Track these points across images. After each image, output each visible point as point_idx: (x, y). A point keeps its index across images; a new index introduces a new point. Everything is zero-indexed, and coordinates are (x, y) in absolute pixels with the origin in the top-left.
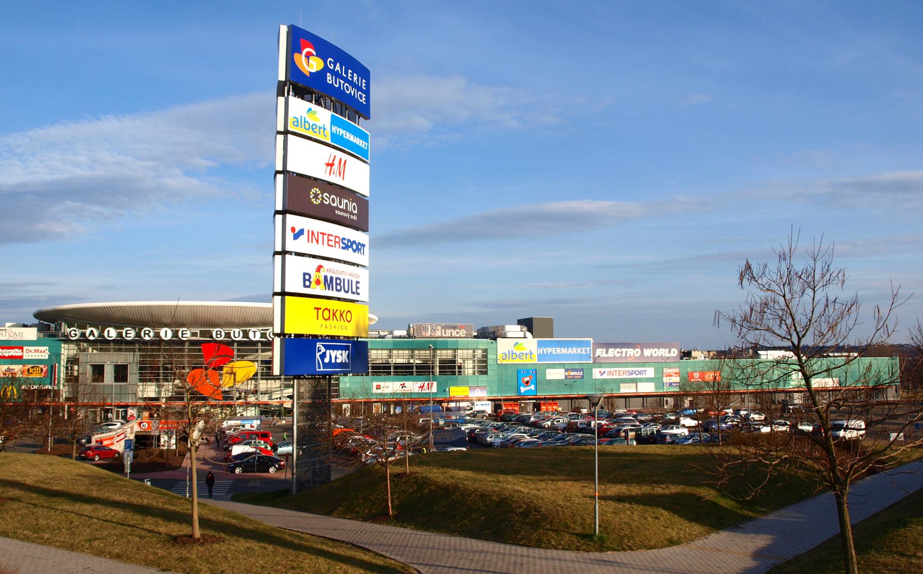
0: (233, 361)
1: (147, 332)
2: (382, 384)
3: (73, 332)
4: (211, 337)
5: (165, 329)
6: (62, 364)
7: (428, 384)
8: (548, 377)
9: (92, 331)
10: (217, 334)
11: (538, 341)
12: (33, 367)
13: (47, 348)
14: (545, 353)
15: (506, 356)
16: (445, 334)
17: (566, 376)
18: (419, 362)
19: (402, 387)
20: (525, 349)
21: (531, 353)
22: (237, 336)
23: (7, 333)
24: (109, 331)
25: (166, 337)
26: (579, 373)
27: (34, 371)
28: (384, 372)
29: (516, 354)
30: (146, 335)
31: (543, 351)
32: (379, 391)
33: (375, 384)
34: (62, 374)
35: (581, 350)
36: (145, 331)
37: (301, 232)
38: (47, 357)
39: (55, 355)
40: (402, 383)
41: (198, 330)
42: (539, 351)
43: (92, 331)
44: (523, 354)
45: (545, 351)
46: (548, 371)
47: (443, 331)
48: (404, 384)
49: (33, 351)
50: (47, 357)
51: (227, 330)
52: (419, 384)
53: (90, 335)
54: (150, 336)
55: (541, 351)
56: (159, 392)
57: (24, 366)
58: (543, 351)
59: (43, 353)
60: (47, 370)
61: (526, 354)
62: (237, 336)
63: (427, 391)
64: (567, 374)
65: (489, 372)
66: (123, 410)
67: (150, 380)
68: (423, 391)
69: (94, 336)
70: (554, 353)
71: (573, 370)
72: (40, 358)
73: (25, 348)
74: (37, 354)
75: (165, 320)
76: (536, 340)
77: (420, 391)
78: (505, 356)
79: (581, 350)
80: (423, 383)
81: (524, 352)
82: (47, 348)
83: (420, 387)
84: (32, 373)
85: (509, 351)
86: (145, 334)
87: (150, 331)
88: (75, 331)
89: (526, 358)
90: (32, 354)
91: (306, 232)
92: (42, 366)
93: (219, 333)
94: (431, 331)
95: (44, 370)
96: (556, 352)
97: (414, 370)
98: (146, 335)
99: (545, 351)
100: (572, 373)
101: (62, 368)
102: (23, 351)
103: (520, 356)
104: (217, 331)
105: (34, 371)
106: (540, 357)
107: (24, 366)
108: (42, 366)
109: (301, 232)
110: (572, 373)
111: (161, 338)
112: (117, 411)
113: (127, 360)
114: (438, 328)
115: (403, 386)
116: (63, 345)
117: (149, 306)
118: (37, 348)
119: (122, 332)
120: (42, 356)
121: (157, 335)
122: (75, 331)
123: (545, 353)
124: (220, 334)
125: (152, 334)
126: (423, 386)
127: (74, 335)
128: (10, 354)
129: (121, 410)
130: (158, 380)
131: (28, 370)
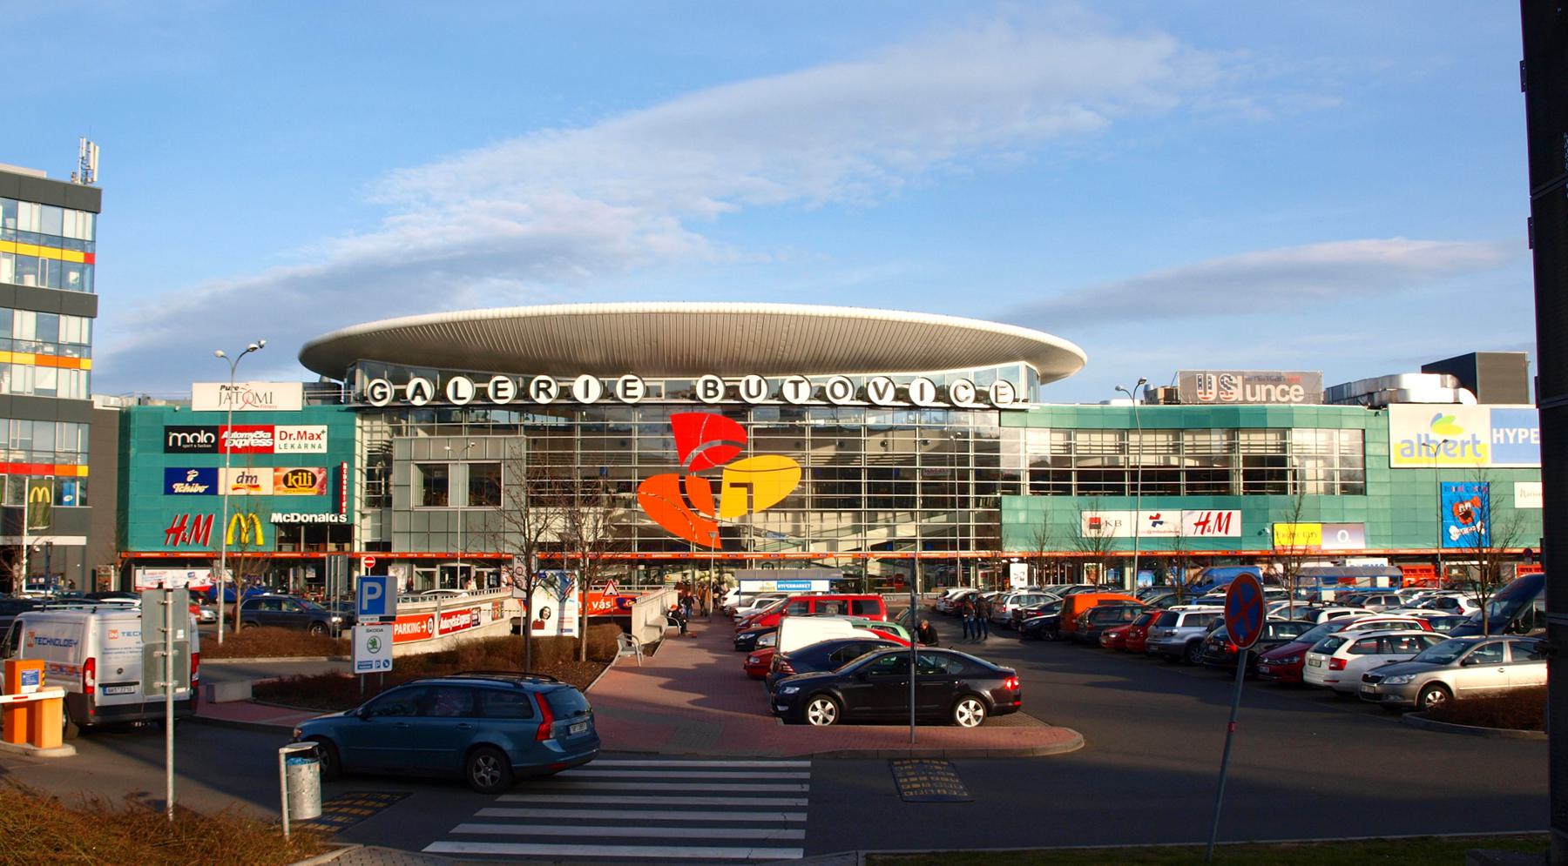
0: (745, 456)
1: (543, 385)
2: (1104, 515)
3: (378, 390)
4: (694, 396)
5: (584, 378)
6: (358, 465)
7: (1220, 516)
9: (419, 386)
10: (706, 389)
11: (1492, 410)
12: (295, 473)
13: (325, 428)
14: (1511, 441)
15: (1411, 448)
16: (1253, 395)
18: (1189, 463)
19: (1154, 525)
21: (1476, 442)
22: (753, 391)
23: (240, 396)
24: (456, 383)
25: (587, 395)
27: (297, 480)
28: (1107, 487)
30: (541, 393)
31: (1506, 435)
33: (1088, 515)
34: (357, 488)
36: (539, 382)
38: (324, 450)
39: (342, 445)
40: (1154, 514)
41: (660, 382)
42: (1495, 435)
43: (419, 386)
45: (1511, 436)
47: (1248, 387)
48: (1158, 516)
49: (295, 436)
50: (324, 450)
51: (731, 380)
52: (1197, 515)
53: (415, 394)
54: (549, 396)
55: (1501, 435)
56: (576, 528)
57: (276, 470)
58: (1506, 435)
59: (313, 440)
60: (324, 480)
61: (1464, 444)
62: (753, 391)
63: (1217, 534)
65: (1369, 492)
66: (491, 570)
67: (553, 502)
68: (1206, 534)
69: (424, 397)
72: (310, 450)
73: (278, 429)
74: (303, 442)
75: (586, 357)
76: (1487, 408)
77: (1198, 534)
80: (1206, 512)
81: (1458, 438)
82: (325, 428)
83: (1197, 524)
84: (293, 487)
86: (538, 389)
87: (549, 384)
88: (383, 386)
89: (1463, 454)
90: (292, 442)
92: (314, 470)
93: (710, 385)
94: (1219, 389)
95: (319, 478)
97: (1183, 482)
98: (541, 393)
99: (1511, 436)
101: (358, 473)
102: (273, 437)
104: (706, 382)
105: (297, 480)
106: (1497, 450)
107: (276, 470)
108: (314, 470)
111: (575, 399)
113: (498, 453)
114: (1234, 381)
115: (1156, 521)
116: (358, 422)
117: (544, 316)
118: (302, 428)
119: (486, 389)
120: (313, 446)
121: (566, 392)
122: (383, 386)
123: (1511, 441)
124: (714, 389)
125: (553, 391)
126: (1207, 521)
127: (379, 397)
128: (247, 444)
129: (487, 570)
130: (571, 502)
131: (286, 480)
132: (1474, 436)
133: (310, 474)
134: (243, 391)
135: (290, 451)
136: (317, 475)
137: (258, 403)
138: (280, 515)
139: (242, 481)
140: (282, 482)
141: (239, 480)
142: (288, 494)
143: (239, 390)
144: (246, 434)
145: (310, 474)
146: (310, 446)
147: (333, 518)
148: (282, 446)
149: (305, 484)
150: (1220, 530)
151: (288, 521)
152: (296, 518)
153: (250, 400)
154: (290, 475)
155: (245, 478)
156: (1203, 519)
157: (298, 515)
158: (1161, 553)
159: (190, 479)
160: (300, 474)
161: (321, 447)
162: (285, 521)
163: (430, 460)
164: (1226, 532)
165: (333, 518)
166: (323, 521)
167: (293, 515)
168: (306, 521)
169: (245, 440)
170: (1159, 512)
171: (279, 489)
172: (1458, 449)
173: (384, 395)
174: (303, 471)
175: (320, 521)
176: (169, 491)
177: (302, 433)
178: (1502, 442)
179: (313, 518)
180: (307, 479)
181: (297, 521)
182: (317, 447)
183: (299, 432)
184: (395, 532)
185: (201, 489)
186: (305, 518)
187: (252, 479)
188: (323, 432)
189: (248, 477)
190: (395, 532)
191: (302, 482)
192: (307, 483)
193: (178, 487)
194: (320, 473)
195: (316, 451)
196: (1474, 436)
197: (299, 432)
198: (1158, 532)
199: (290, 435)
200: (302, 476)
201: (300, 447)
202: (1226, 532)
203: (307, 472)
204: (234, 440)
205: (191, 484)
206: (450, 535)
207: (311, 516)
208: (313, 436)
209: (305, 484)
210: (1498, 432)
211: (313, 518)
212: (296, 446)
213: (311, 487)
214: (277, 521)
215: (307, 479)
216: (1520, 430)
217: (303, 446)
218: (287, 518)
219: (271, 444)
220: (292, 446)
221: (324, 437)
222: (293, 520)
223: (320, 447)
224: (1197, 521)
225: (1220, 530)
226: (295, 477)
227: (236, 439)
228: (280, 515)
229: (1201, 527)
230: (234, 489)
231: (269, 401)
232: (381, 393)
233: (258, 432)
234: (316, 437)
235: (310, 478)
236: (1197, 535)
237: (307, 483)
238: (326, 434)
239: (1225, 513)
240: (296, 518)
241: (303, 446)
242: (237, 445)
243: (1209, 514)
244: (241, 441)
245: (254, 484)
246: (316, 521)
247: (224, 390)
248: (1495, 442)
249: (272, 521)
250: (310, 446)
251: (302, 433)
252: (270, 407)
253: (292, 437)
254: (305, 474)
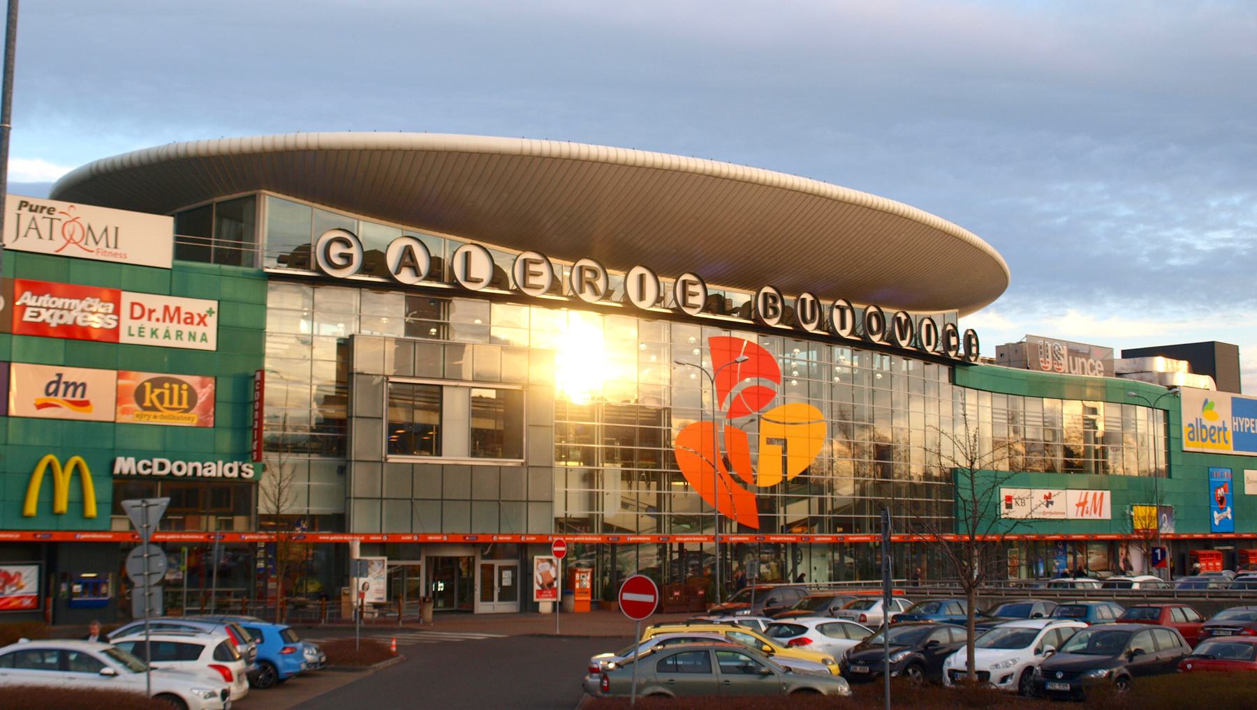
5: (638, 271)
7: (1095, 495)
12: (156, 383)
13: (214, 305)
23: (57, 226)
27: (161, 397)
30: (587, 289)
38: (211, 345)
40: (1046, 492)
49: (159, 314)
50: (211, 345)
72: (185, 343)
73: (127, 298)
74: (174, 327)
82: (214, 305)
83: (1078, 505)
84: (154, 408)
90: (154, 325)
102: (117, 311)
105: (161, 397)
107: (119, 377)
108: (192, 380)
112: (483, 567)
118: (173, 302)
120: (192, 336)
126: (1086, 502)
127: (338, 261)
128: (68, 319)
131: (139, 395)
133: (185, 387)
134: (65, 218)
135: (148, 340)
136: (198, 390)
137: (92, 245)
138: (132, 460)
139: (56, 392)
140: (133, 398)
141: (53, 387)
142: (144, 421)
143: (56, 215)
144: (67, 301)
145: (185, 387)
146: (185, 336)
147: (231, 470)
148: (135, 331)
149: (175, 405)
150: (1095, 512)
151: (148, 471)
152: (162, 466)
153: (77, 237)
154: (148, 385)
155: (62, 387)
156: (1082, 500)
157: (167, 462)
158: (1051, 537)
160: (167, 385)
161: (206, 338)
162: (142, 471)
163: (414, 377)
164: (1100, 515)
165: (231, 470)
166: (213, 474)
167: (156, 461)
168: (182, 473)
169: (65, 312)
170: (1052, 491)
171: (125, 411)
173: (348, 258)
174: (172, 381)
175: (206, 474)
177: (172, 311)
179: (195, 469)
180: (180, 396)
181: (166, 472)
182: (198, 337)
183: (167, 308)
184: (355, 498)
186: (180, 468)
187: (76, 388)
188: (210, 312)
189: (67, 385)
190: (355, 498)
191: (171, 402)
192: (180, 403)
194: (203, 386)
195: (197, 345)
197: (167, 308)
198: (1051, 513)
199: (151, 311)
200: (171, 389)
201: (167, 335)
202: (1100, 515)
203: (180, 383)
204: (43, 311)
206: (440, 502)
207: (191, 465)
208: (192, 317)
209: (175, 405)
211: (195, 469)
212: (161, 333)
213: (186, 411)
214: (125, 471)
215: (180, 396)
217: (173, 334)
218: (145, 467)
219: (114, 324)
220: (154, 333)
221: (212, 321)
222: (156, 471)
223: (204, 338)
224: (1077, 502)
225: (1095, 512)
226: (157, 391)
227: (48, 309)
228: (132, 460)
229: (1081, 508)
230: (40, 407)
231: (112, 244)
232: (342, 255)
233: (89, 300)
234: (197, 319)
235: (185, 394)
236: (1078, 518)
237: (180, 403)
238: (215, 316)
239: (1099, 492)
240: (162, 466)
241: (173, 334)
242: (48, 320)
243: (1087, 493)
244: (58, 313)
245: (78, 398)
246: (199, 474)
247: (25, 210)
249: (117, 471)
250: (185, 336)
251: (172, 311)
252: (115, 255)
253: (154, 316)
254: (176, 387)
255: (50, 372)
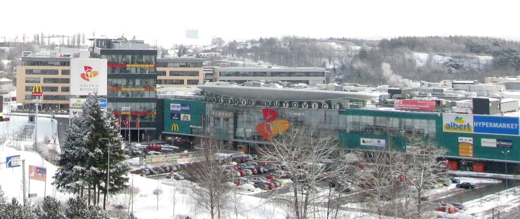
2: (365, 140)
8: (483, 145)
14: (480, 126)
17: (498, 145)
19: (378, 143)
20: (464, 122)
26: (508, 143)
29: (457, 126)
31: (478, 125)
32: (364, 144)
33: (362, 139)
35: (510, 126)
37: (76, 112)
42: (475, 124)
44: (462, 125)
46: (482, 140)
55: (477, 124)
61: (465, 126)
64: (498, 143)
69: (215, 101)
70: (487, 126)
71: (504, 141)
78: (448, 126)
79: (510, 126)
81: (463, 124)
85: (451, 123)
91: (78, 112)
96: (489, 126)
100: (502, 143)
103: (460, 127)
106: (476, 129)
109: (76, 112)
110: (502, 143)
123: (480, 126)
132: (468, 124)
159: (175, 116)
172: (463, 127)
176: (171, 118)
178: (477, 125)
185: (177, 118)
193: (174, 118)
196: (468, 124)
205: (175, 117)
210: (476, 123)
216: (483, 123)
248: (475, 125)
255: (184, 115)
